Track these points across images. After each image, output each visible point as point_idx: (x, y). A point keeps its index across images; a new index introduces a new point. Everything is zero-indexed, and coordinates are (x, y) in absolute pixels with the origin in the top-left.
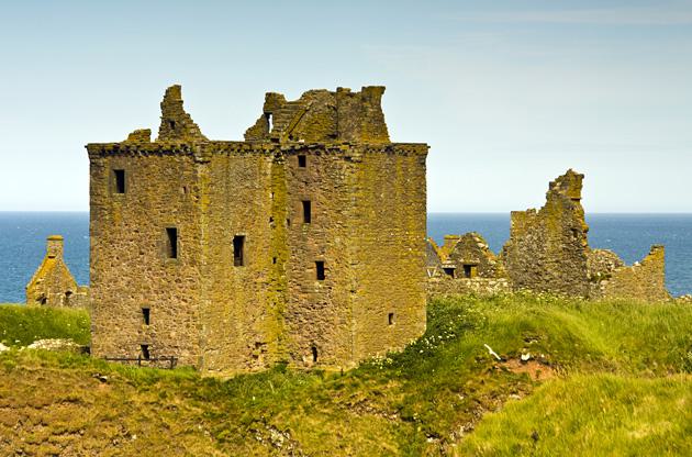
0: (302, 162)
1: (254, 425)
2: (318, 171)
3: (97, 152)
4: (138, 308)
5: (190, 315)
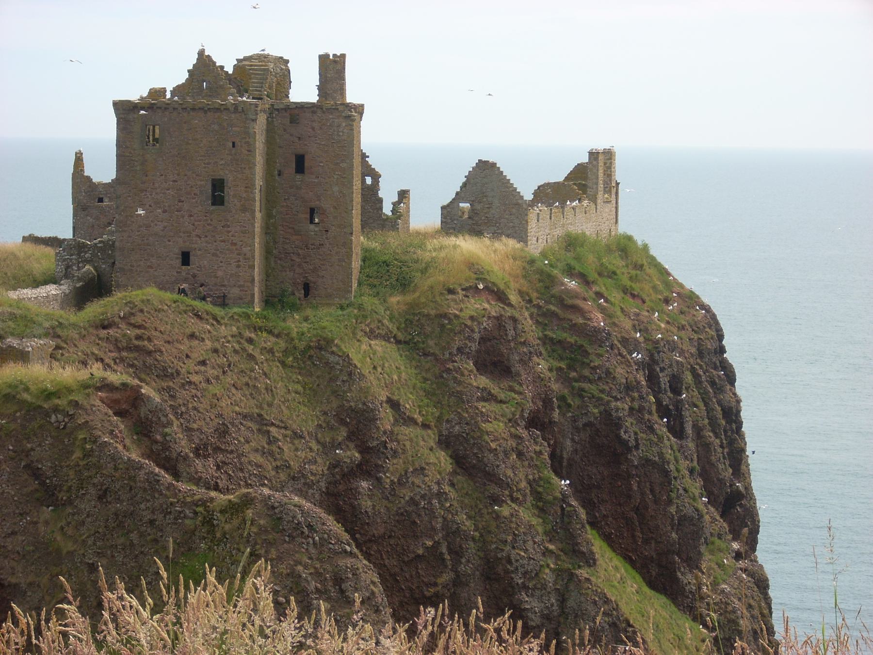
0: (294, 120)
1: (312, 352)
2: (313, 129)
3: (125, 110)
4: (176, 250)
5: (241, 258)
